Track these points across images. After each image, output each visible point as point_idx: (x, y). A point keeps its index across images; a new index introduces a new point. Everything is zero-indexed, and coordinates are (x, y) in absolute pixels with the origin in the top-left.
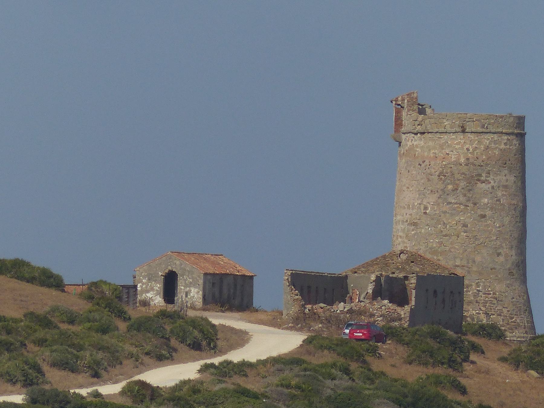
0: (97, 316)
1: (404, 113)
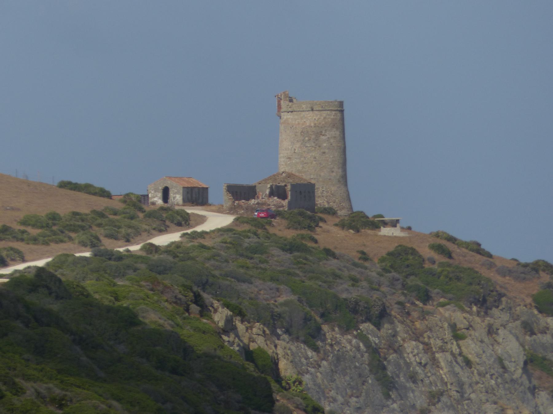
0: (128, 211)
1: (282, 102)
